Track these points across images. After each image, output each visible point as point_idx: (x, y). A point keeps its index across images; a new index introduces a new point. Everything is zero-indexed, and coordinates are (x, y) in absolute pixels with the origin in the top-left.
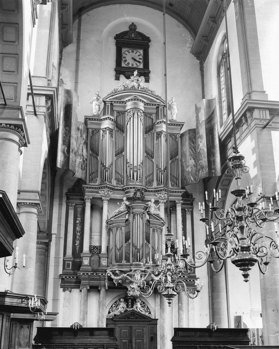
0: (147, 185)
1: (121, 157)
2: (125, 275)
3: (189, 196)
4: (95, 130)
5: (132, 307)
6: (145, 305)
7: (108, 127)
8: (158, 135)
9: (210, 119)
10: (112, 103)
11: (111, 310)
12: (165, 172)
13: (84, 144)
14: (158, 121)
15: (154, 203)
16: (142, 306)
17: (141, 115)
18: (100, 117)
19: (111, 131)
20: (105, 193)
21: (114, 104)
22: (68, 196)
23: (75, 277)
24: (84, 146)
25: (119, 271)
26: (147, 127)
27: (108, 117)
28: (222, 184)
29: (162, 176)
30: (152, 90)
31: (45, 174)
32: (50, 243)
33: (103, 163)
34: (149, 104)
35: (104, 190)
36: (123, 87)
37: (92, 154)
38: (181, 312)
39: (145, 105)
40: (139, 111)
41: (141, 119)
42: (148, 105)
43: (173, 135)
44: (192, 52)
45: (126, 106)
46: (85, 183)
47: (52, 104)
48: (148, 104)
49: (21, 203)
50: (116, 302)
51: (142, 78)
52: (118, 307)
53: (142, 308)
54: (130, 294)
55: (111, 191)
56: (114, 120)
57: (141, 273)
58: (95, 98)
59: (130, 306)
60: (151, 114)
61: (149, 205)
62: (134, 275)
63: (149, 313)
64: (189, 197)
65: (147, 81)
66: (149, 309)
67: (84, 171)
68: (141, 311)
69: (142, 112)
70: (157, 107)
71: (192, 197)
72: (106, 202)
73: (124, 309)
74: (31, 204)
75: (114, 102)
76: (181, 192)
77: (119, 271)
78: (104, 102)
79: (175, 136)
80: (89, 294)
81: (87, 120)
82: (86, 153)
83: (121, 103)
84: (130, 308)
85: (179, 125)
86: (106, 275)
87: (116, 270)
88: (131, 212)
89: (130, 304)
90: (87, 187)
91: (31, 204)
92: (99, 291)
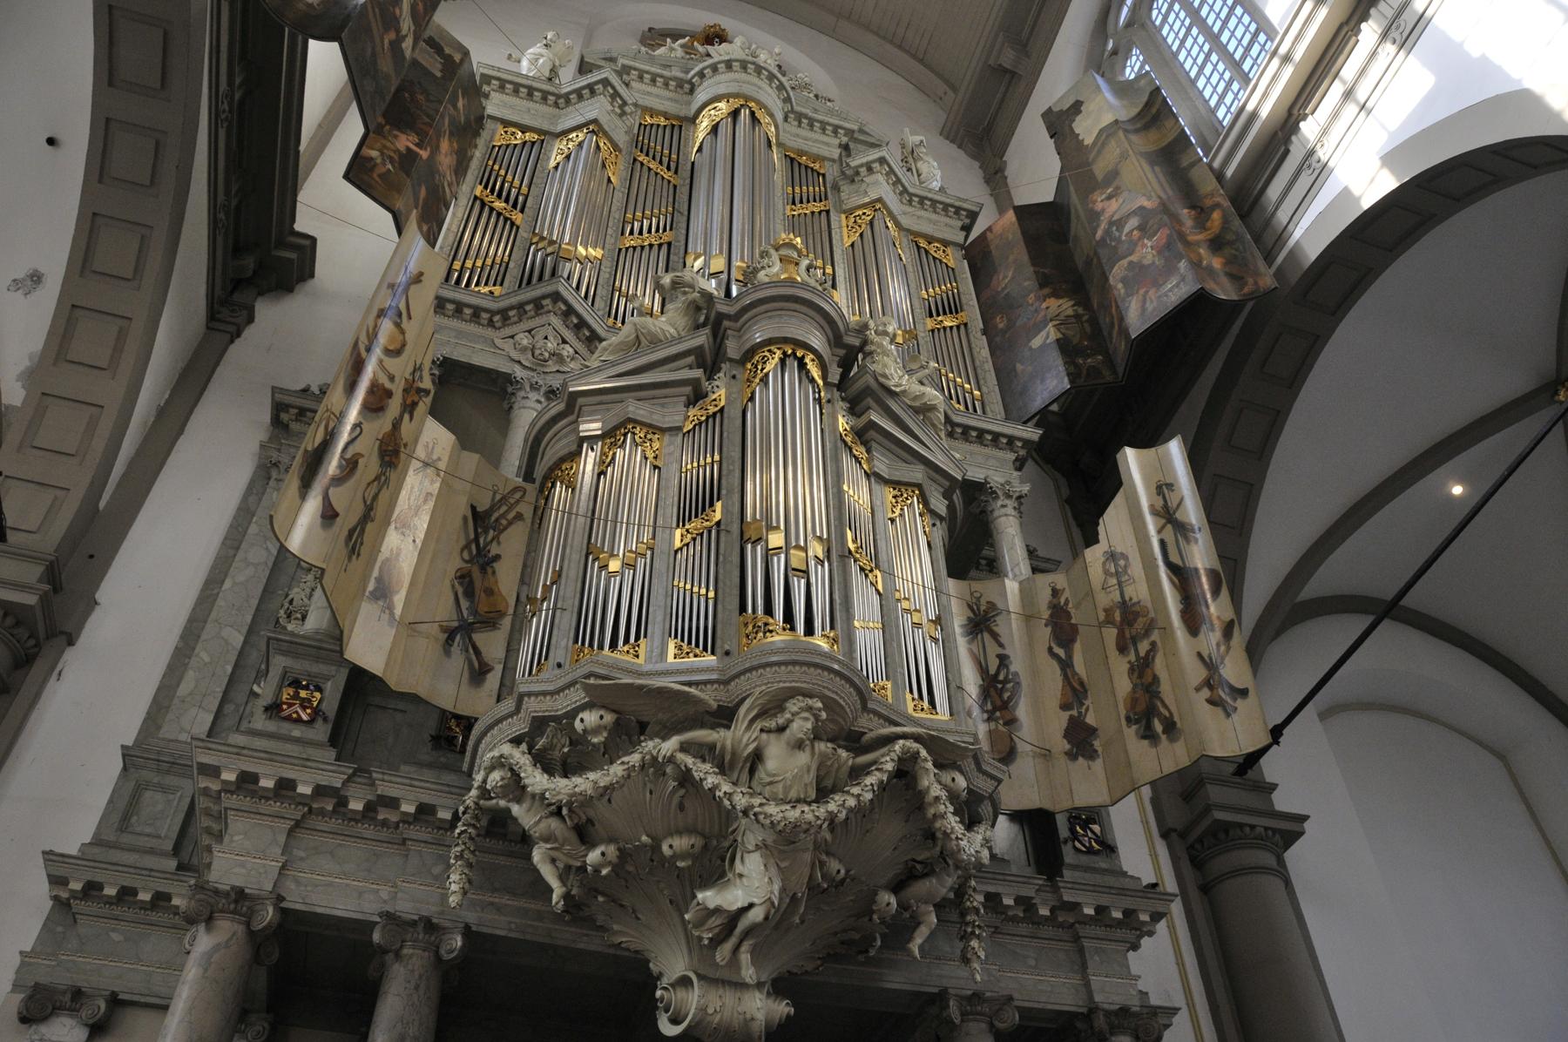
2: (669, 746)
7: (595, 121)
20: (538, 345)
21: (633, 84)
22: (284, 417)
34: (806, 117)
35: (529, 331)
37: (486, 199)
42: (799, 126)
48: (800, 117)
54: (675, 1021)
55: (576, 353)
57: (822, 746)
62: (757, 757)
72: (534, 396)
76: (1011, 440)
85: (958, 210)
88: (733, 348)
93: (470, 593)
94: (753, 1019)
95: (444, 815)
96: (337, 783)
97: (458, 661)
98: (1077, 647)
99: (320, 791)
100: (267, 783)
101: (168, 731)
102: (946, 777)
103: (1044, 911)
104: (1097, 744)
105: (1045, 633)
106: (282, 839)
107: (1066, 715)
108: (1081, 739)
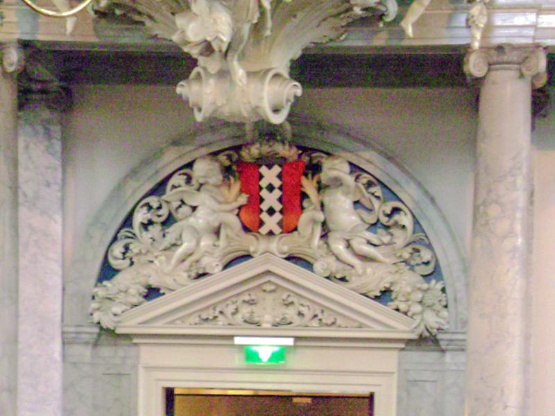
5: (289, 229)
6: (396, 210)
11: (118, 249)
50: (159, 189)
52: (173, 231)
53: (369, 235)
59: (271, 223)
66: (429, 246)
68: (364, 258)
84: (271, 233)
89: (271, 199)
94: (257, 107)
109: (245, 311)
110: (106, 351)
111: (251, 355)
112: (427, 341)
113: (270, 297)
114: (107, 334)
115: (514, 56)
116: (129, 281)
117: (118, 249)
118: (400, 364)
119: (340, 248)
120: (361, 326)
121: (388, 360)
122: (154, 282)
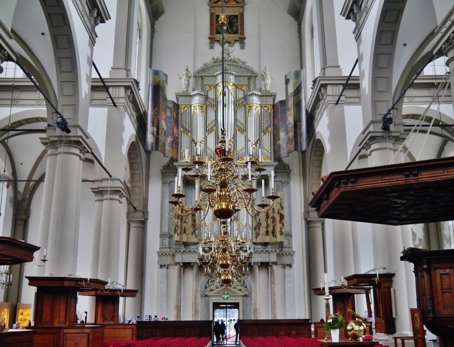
0: (238, 159)
1: (213, 132)
3: (286, 167)
4: (186, 106)
8: (250, 107)
9: (298, 91)
10: (203, 77)
11: (207, 285)
12: (256, 145)
13: (174, 122)
14: (249, 94)
15: (242, 179)
16: (238, 280)
17: (231, 88)
18: (190, 93)
19: (202, 106)
21: (204, 78)
23: (171, 254)
24: (175, 124)
25: (208, 247)
26: (239, 99)
27: (198, 93)
28: (315, 154)
29: (254, 150)
30: (243, 61)
31: (137, 154)
32: (147, 221)
33: (194, 140)
36: (213, 60)
38: (273, 286)
39: (236, 77)
40: (229, 84)
41: (231, 93)
43: (265, 106)
44: (288, 12)
45: (216, 79)
46: (177, 161)
47: (132, 92)
48: (238, 76)
49: (104, 191)
51: (237, 45)
52: (214, 282)
53: (238, 283)
56: (205, 94)
58: (185, 73)
60: (242, 86)
61: (236, 182)
63: (245, 288)
64: (286, 169)
65: (242, 48)
66: (245, 284)
67: (176, 150)
68: (238, 285)
69: (232, 84)
70: (248, 78)
71: (289, 169)
73: (220, 284)
74: (112, 191)
75: (204, 76)
76: (273, 165)
77: (208, 247)
78: (195, 77)
79: (267, 107)
80: (185, 270)
81: (178, 96)
82: (177, 131)
83: (212, 76)
85: (271, 96)
86: (198, 252)
87: (205, 247)
90: (179, 165)
91: (112, 191)
92: (192, 267)
93: (194, 226)
95: (196, 251)
96: (185, 250)
97: (194, 236)
98: (269, 219)
99: (183, 251)
100: (178, 251)
101: (163, 231)
102: (243, 249)
103: (264, 251)
104: (269, 234)
105: (266, 216)
106: (181, 255)
107: (266, 230)
108: (267, 233)
109: (223, 292)
110: (206, 298)
111: (224, 298)
112: (246, 296)
113: (226, 291)
114: (206, 296)
115: (256, 263)
116: (209, 289)
117: (207, 285)
118: (242, 299)
119: (234, 284)
120: (237, 294)
121: (241, 298)
122: (212, 289)
